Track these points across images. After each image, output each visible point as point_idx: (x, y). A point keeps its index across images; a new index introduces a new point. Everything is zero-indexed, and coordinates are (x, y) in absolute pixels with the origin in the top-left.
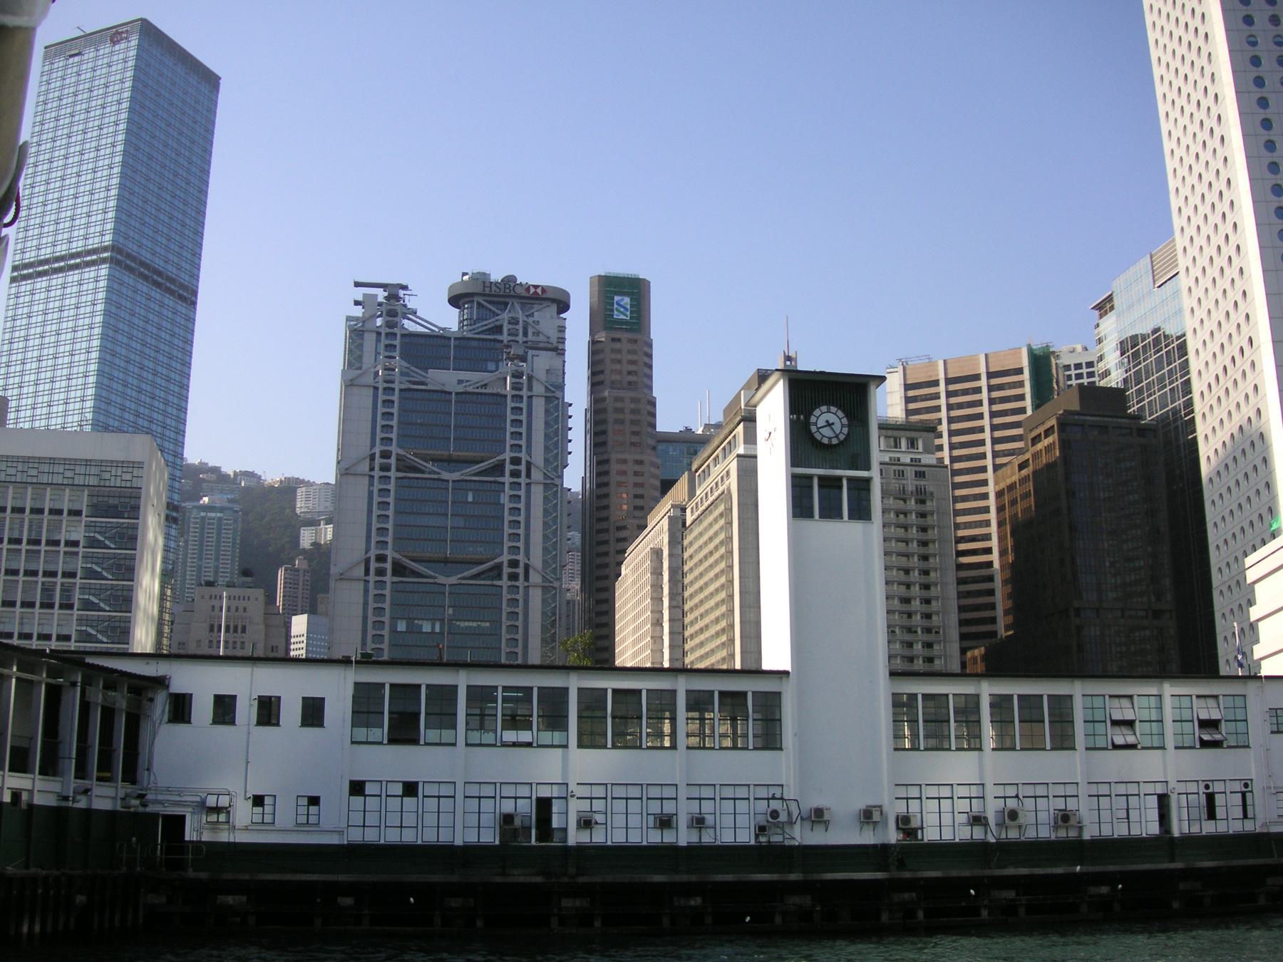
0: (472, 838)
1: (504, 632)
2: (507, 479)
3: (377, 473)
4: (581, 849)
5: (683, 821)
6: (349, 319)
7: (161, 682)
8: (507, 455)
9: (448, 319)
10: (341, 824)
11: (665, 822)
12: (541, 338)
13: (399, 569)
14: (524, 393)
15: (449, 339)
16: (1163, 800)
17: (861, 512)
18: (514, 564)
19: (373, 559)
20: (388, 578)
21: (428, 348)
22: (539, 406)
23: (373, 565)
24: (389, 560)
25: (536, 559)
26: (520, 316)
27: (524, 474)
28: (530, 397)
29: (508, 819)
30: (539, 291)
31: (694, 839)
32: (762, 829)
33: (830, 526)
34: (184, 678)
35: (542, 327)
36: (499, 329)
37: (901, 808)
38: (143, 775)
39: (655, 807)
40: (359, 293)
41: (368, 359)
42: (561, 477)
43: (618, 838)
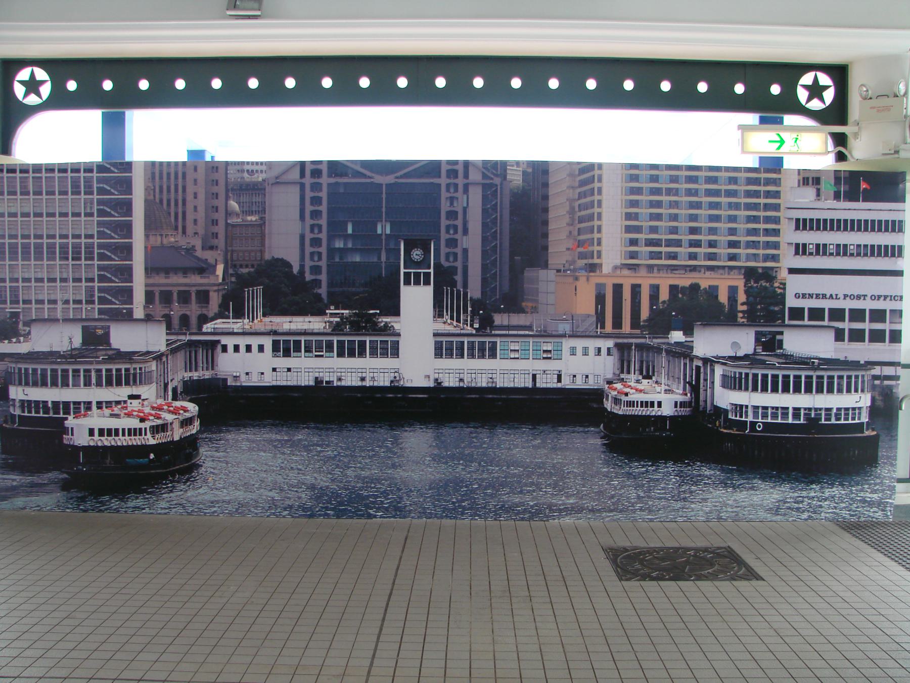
0: (307, 384)
4: (338, 387)
5: (368, 379)
7: (219, 341)
10: (269, 380)
11: (363, 379)
16: (534, 376)
17: (427, 283)
29: (316, 378)
31: (371, 384)
32: (392, 382)
33: (417, 288)
34: (225, 340)
37: (436, 376)
38: (216, 368)
39: (360, 375)
43: (349, 384)
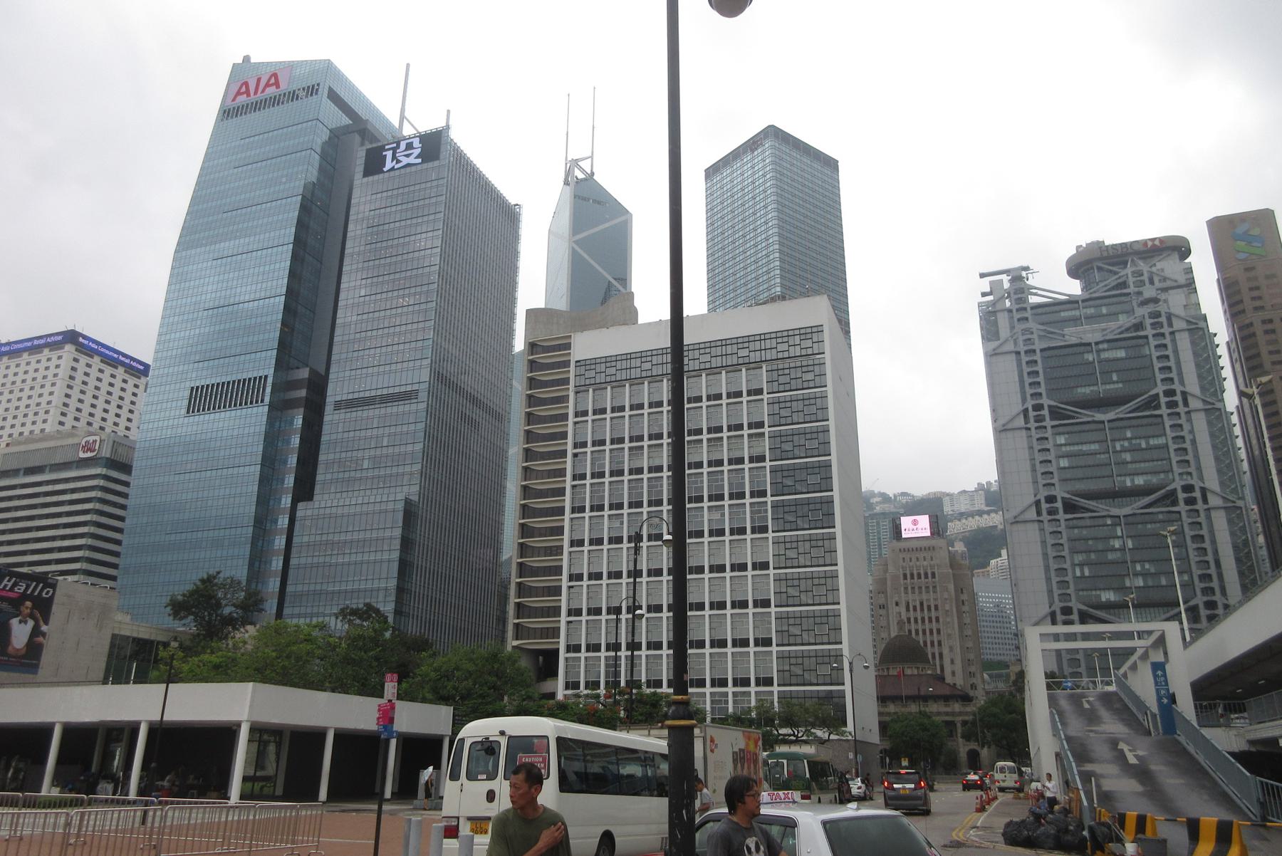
1: (1191, 556)
2: (1164, 411)
3: (1032, 425)
6: (980, 305)
8: (1160, 389)
9: (1074, 288)
12: (1169, 283)
13: (1070, 507)
14: (1166, 330)
15: (1077, 302)
18: (1188, 488)
19: (1043, 501)
20: (1061, 516)
21: (1056, 310)
22: (1184, 342)
23: (1046, 505)
24: (1059, 500)
25: (1212, 482)
26: (1142, 265)
27: (1181, 403)
28: (1172, 333)
30: (1157, 243)
35: (1168, 273)
36: (1124, 285)
40: (985, 285)
41: (1004, 332)
42: (1222, 400)
